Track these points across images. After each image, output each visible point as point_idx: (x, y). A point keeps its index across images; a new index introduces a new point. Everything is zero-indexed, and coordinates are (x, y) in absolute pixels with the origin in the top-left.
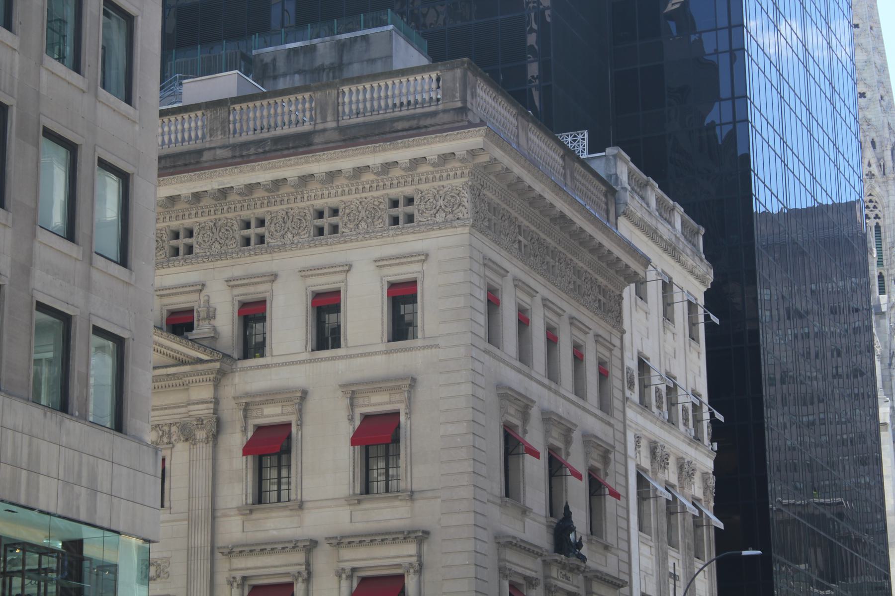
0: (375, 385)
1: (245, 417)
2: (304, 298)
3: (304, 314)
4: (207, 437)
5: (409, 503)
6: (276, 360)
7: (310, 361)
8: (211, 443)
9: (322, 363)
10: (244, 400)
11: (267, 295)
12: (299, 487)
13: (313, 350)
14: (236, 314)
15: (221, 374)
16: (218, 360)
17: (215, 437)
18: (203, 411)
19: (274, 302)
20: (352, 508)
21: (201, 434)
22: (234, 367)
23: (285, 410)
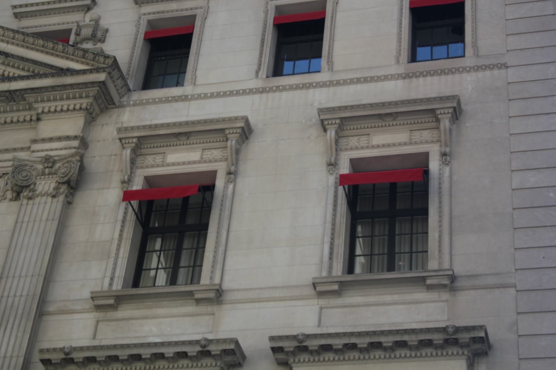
0: (385, 115)
1: (133, 162)
2: (262, 15)
3: (260, 33)
4: (56, 188)
5: (445, 296)
6: (199, 90)
7: (263, 91)
8: (61, 198)
9: (285, 94)
10: (137, 134)
11: (199, 13)
12: (219, 267)
13: (267, 77)
14: (141, 36)
15: (104, 101)
16: (104, 70)
17: (74, 184)
18: (58, 150)
19: (209, 22)
20: (323, 302)
21: (46, 185)
22: (125, 99)
23: (208, 155)
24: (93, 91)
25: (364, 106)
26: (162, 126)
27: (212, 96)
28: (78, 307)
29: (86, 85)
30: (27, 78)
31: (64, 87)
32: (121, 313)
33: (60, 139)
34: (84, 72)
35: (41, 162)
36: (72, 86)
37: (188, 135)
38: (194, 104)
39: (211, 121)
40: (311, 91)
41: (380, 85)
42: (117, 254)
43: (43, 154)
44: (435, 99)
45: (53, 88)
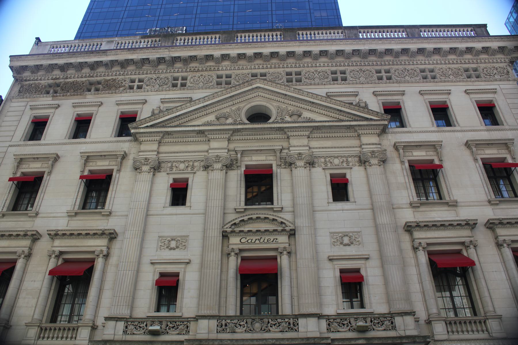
24: (381, 128)
25: (483, 140)
26: (412, 142)
27: (420, 132)
28: (404, 206)
29: (379, 125)
30: (350, 121)
31: (371, 125)
32: (421, 209)
33: (373, 144)
34: (379, 120)
35: (370, 153)
36: (374, 125)
37: (420, 146)
38: (415, 135)
39: (430, 142)
40: (456, 133)
41: (479, 132)
42: (410, 188)
43: (372, 149)
44: (507, 139)
45: (367, 125)
